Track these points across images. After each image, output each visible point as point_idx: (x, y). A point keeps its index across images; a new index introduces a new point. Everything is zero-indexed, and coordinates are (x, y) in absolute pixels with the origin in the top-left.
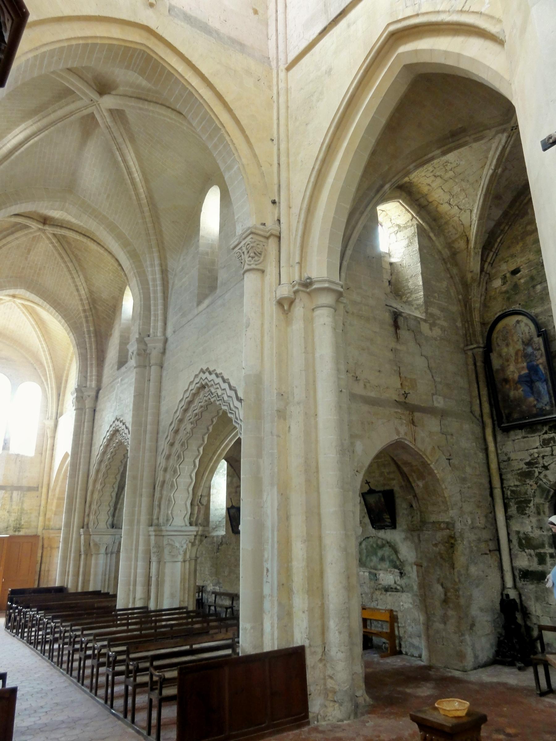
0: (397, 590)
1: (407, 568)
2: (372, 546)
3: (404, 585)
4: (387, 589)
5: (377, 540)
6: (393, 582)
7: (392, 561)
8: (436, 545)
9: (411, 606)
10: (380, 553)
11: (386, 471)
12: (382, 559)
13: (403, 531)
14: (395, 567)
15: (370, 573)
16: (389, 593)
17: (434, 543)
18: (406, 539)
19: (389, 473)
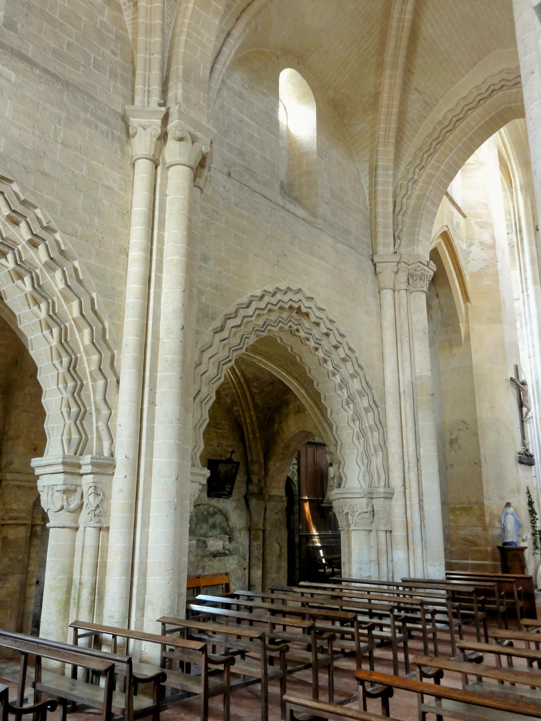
0: (225, 555)
1: (236, 534)
2: (203, 514)
3: (231, 549)
4: (215, 555)
5: (208, 508)
6: (222, 547)
7: (223, 528)
8: (277, 513)
9: (236, 566)
10: (211, 521)
11: (224, 443)
12: (214, 526)
13: (235, 500)
14: (226, 533)
15: (198, 540)
16: (217, 558)
17: (276, 511)
18: (236, 508)
19: (228, 446)
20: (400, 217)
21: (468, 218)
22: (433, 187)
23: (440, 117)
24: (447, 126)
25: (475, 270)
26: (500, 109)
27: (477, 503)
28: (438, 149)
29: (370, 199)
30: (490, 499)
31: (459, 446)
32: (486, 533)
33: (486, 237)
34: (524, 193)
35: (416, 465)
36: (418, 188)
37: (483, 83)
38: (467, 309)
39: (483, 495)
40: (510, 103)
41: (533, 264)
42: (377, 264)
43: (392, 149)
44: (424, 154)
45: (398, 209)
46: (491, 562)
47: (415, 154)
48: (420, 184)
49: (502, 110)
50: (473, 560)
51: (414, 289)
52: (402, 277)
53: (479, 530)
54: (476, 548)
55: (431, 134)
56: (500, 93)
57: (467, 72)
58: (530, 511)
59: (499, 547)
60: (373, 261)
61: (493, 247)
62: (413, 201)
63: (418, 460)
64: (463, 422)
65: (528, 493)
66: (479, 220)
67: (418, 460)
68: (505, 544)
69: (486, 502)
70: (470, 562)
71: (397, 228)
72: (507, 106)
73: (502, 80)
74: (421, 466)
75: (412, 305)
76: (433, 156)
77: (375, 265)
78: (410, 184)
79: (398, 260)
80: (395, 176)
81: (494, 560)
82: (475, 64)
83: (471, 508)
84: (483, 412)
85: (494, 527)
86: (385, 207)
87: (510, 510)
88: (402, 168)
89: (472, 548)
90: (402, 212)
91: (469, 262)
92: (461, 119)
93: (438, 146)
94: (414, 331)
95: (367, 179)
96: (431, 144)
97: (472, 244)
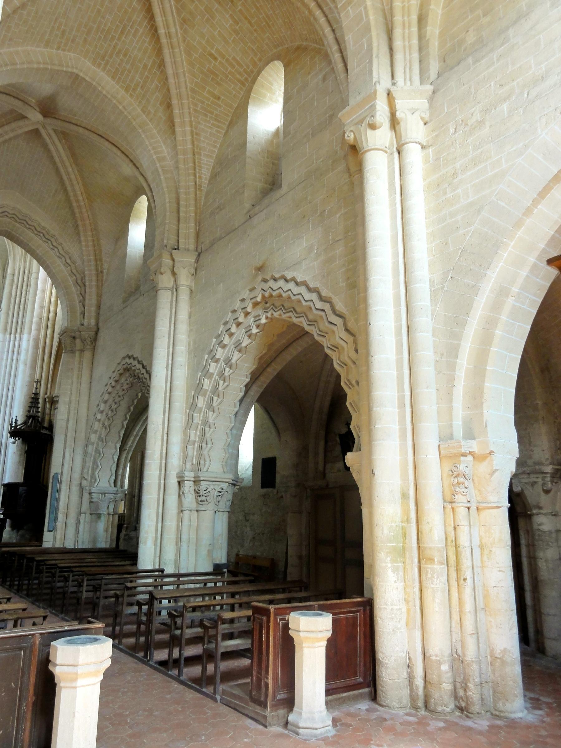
56: (8, 220)
73: (14, 214)
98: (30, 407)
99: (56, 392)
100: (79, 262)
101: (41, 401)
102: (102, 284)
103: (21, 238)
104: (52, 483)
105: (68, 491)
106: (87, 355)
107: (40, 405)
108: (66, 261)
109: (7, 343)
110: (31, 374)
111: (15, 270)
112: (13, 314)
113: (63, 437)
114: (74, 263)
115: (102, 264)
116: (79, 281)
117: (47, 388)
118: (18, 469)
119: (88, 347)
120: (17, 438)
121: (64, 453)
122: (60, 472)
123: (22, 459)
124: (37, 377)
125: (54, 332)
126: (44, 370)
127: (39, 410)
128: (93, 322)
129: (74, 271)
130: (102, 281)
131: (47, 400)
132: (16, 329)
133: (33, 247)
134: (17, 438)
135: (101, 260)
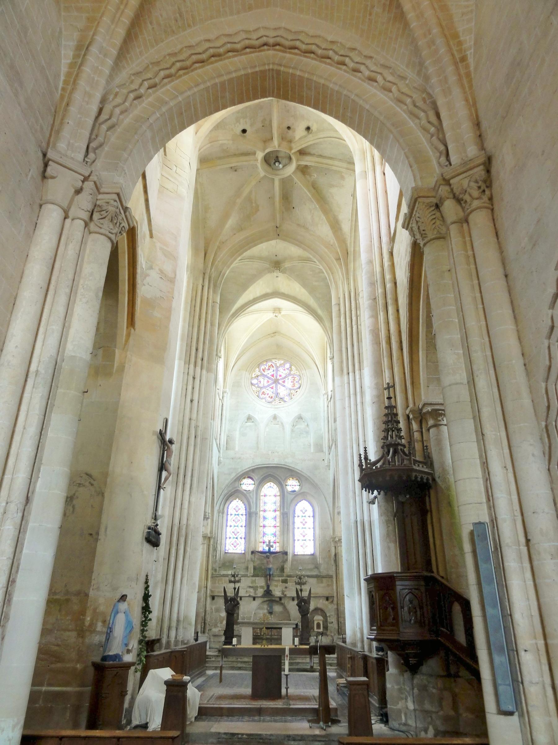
20: (104, 127)
21: (154, 240)
22: (161, 115)
23: (193, 42)
24: (200, 54)
25: (149, 296)
26: (267, 67)
27: (78, 593)
28: (180, 76)
29: (66, 82)
30: (98, 589)
31: (74, 507)
32: (80, 640)
33: (168, 268)
34: (189, 273)
35: (21, 507)
36: (139, 108)
37: (254, 31)
38: (128, 335)
39: (90, 582)
40: (281, 65)
41: (182, 340)
42: (50, 163)
43: (121, 32)
44: (160, 70)
45: (104, 117)
46: (78, 689)
47: (148, 66)
48: (144, 105)
49: (269, 70)
50: (50, 685)
51: (97, 229)
52: (84, 202)
53: (71, 637)
54: (59, 665)
55: (176, 53)
56: (271, 52)
57: (238, 12)
58: (143, 608)
59: (95, 665)
60: (45, 155)
61: (172, 281)
62: (128, 120)
63: (28, 500)
64: (87, 474)
65: (146, 582)
66: (165, 248)
67: (28, 500)
68: (104, 658)
69: (92, 593)
70: (44, 689)
71: (95, 139)
72: (276, 67)
74: (29, 513)
75: (88, 251)
76: (173, 81)
77: (46, 165)
78: (132, 96)
79: (87, 174)
80: (111, 77)
81: (83, 685)
82: (250, 8)
83: (68, 600)
84: (119, 466)
85: (94, 631)
86: (86, 99)
87: (123, 606)
88: (123, 75)
89: (53, 666)
90: (109, 123)
91: (144, 285)
92: (219, 55)
93: (181, 72)
94: (80, 286)
95: (71, 54)
96: (173, 64)
97: (151, 268)
98: (387, 431)
99: (423, 398)
100: (411, 74)
101: (401, 418)
102: (470, 82)
103: (298, 73)
104: (474, 552)
105: (528, 575)
106: (480, 219)
107: (402, 425)
108: (385, 79)
109: (346, 385)
110: (377, 384)
111: (339, 298)
112: (347, 349)
113: (470, 425)
114: (403, 78)
115: (460, 43)
116: (420, 103)
117: (407, 399)
118: (389, 548)
119: (476, 203)
120: (376, 492)
121: (485, 465)
122: (486, 519)
123: (391, 528)
124: (387, 379)
125: (398, 311)
126: (396, 369)
127: (403, 434)
128: (472, 151)
129: (405, 90)
130: (468, 75)
131: (411, 416)
132: (354, 365)
133: (322, 81)
134: (376, 492)
135: (456, 36)
